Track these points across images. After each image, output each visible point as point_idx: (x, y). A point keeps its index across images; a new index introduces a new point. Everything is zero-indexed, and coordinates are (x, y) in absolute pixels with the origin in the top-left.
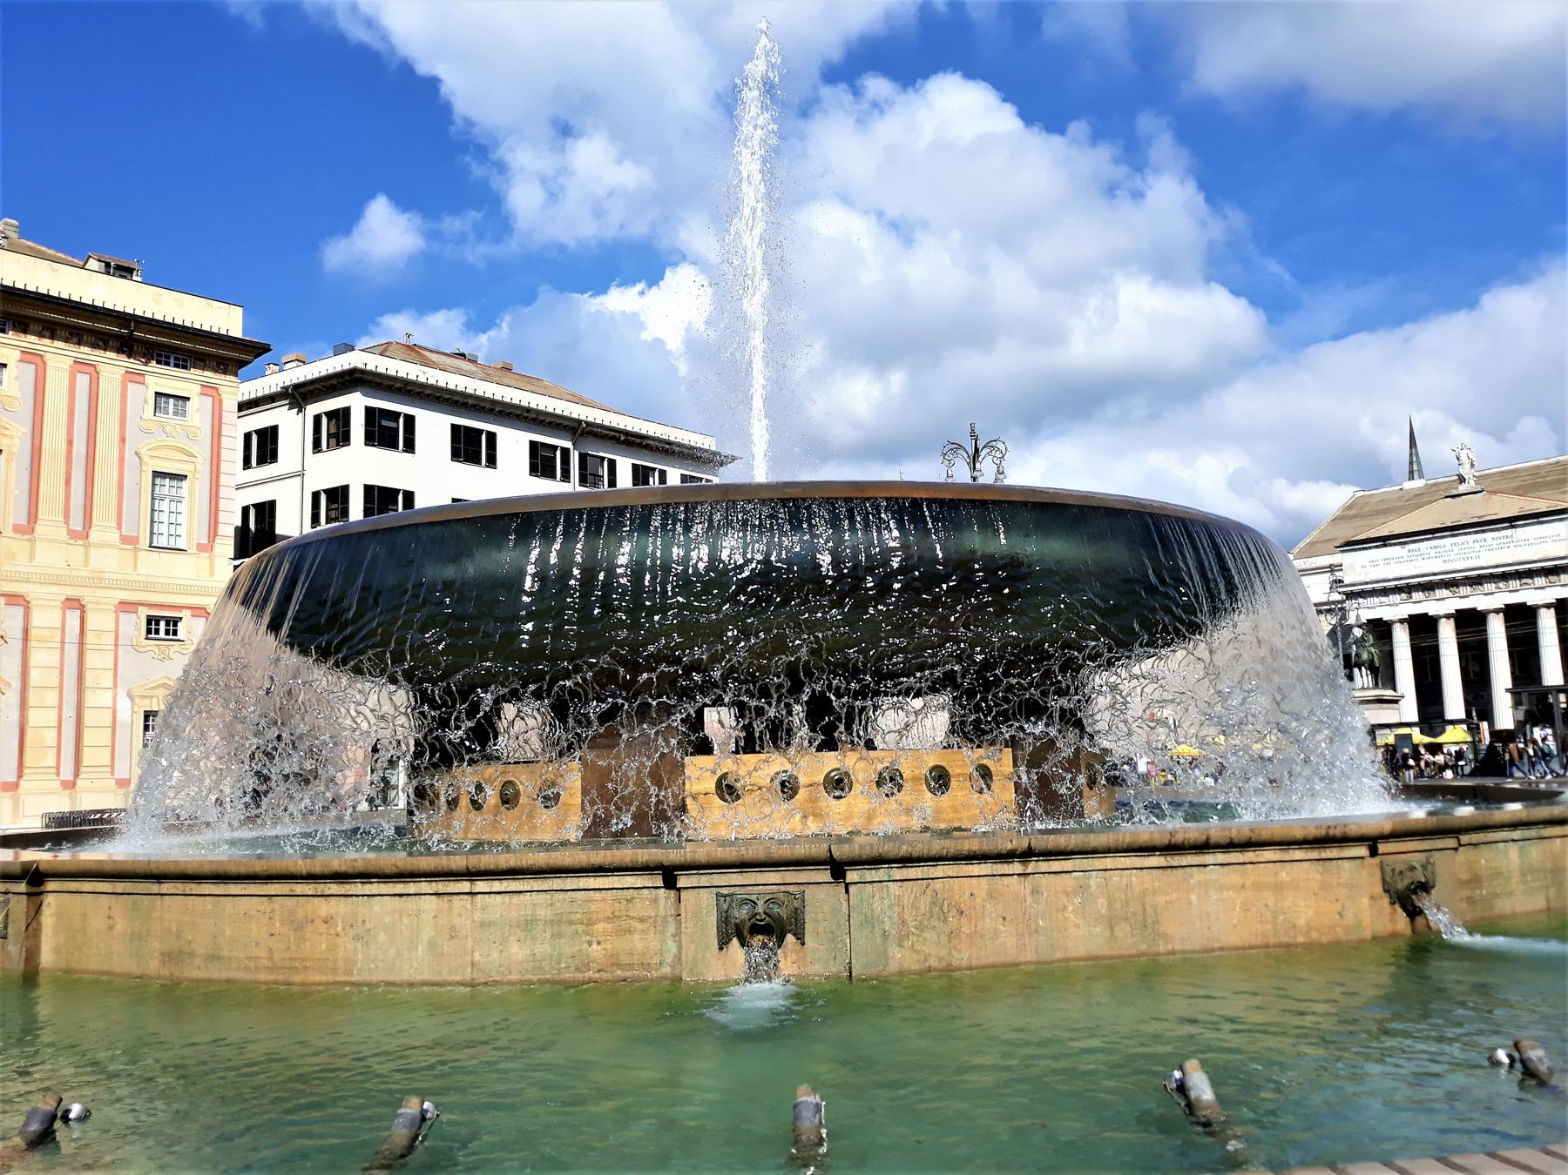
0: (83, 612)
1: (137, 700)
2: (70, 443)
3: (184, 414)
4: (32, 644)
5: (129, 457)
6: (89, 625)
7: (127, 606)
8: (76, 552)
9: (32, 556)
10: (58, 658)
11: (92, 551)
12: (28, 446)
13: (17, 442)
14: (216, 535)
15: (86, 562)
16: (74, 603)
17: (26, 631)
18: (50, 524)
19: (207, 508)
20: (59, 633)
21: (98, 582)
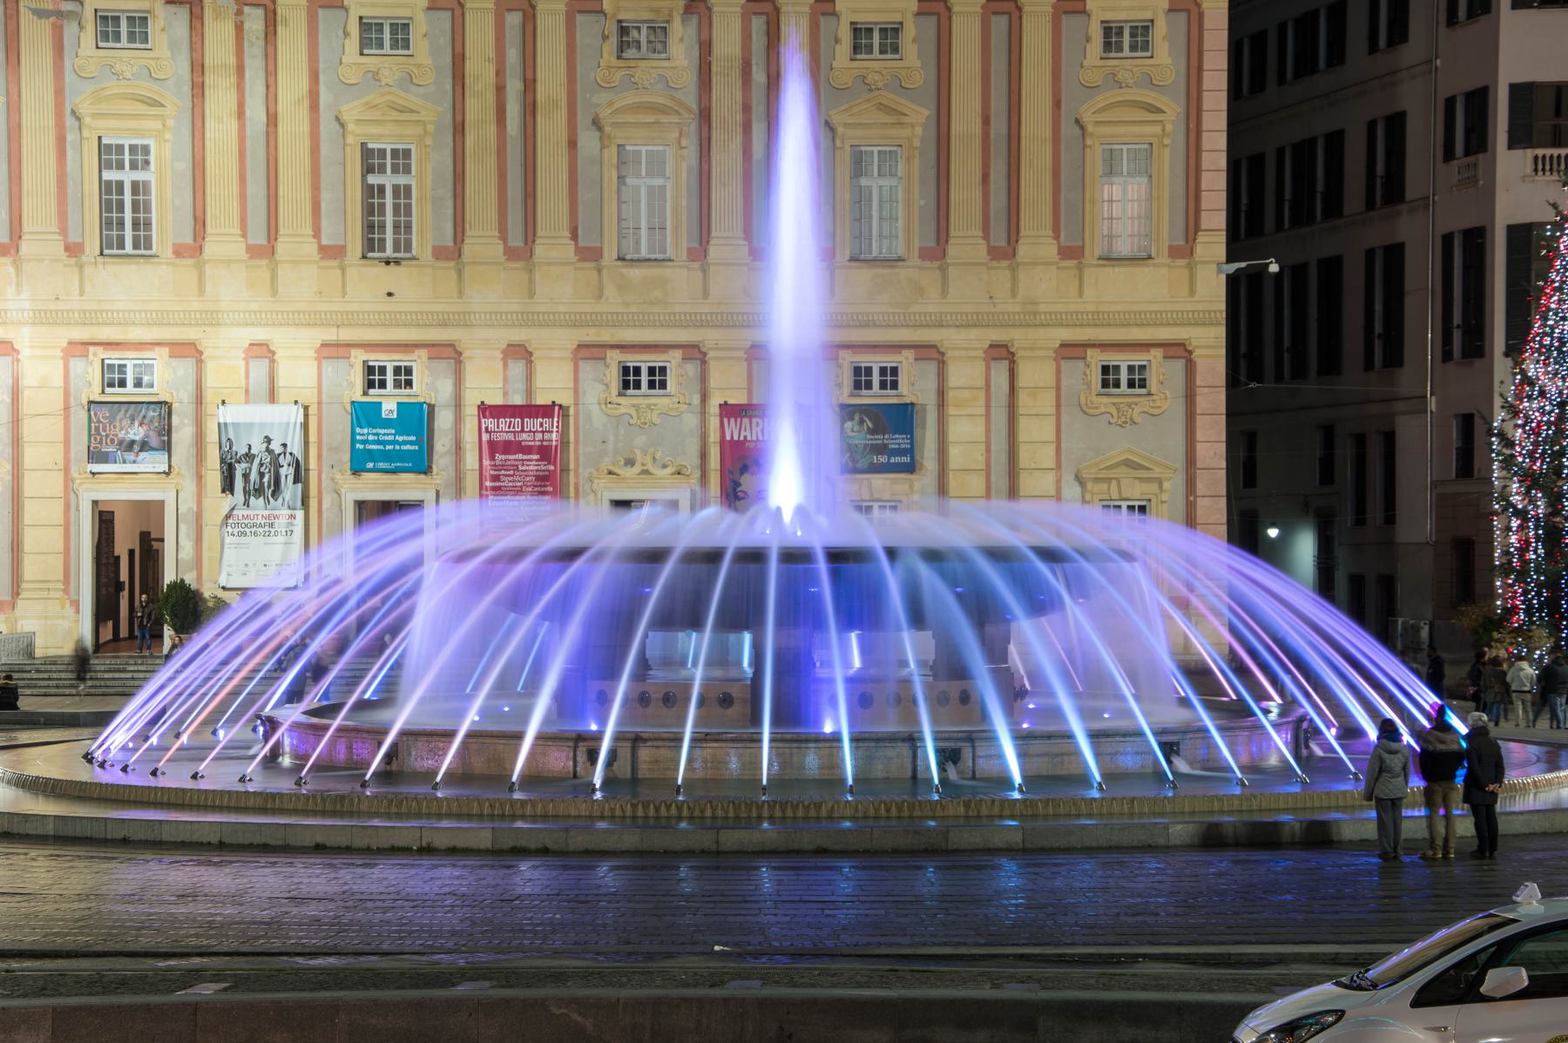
0: (1012, 362)
1: (1089, 485)
2: (986, 121)
3: (1145, 47)
4: (951, 411)
5: (1068, 129)
6: (1023, 379)
7: (1071, 351)
8: (1000, 274)
9: (944, 292)
10: (981, 429)
11: (1022, 275)
12: (933, 133)
13: (919, 130)
14: (1197, 229)
15: (1014, 293)
16: (1002, 353)
17: (941, 393)
18: (967, 243)
19: (1181, 189)
20: (982, 394)
21: (1031, 319)
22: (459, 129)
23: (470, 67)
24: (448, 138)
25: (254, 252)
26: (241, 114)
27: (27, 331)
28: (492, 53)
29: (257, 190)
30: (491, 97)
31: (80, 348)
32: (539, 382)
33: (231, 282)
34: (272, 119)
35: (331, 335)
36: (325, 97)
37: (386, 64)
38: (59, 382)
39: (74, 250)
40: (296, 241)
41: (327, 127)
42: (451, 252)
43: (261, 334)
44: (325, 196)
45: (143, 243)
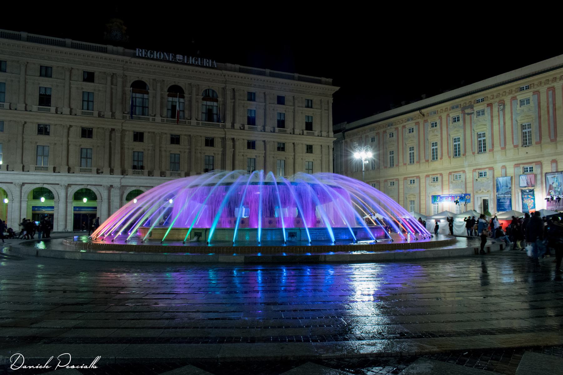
22: (540, 117)
23: (541, 104)
24: (537, 120)
25: (502, 149)
26: (499, 124)
27: (467, 168)
28: (546, 100)
29: (502, 137)
30: (546, 109)
31: (474, 170)
32: (559, 167)
33: (499, 155)
34: (504, 123)
35: (516, 162)
36: (514, 117)
37: (525, 107)
38: (472, 176)
39: (474, 153)
40: (510, 145)
41: (514, 122)
42: (539, 143)
43: (504, 164)
44: (514, 136)
45: (485, 150)
